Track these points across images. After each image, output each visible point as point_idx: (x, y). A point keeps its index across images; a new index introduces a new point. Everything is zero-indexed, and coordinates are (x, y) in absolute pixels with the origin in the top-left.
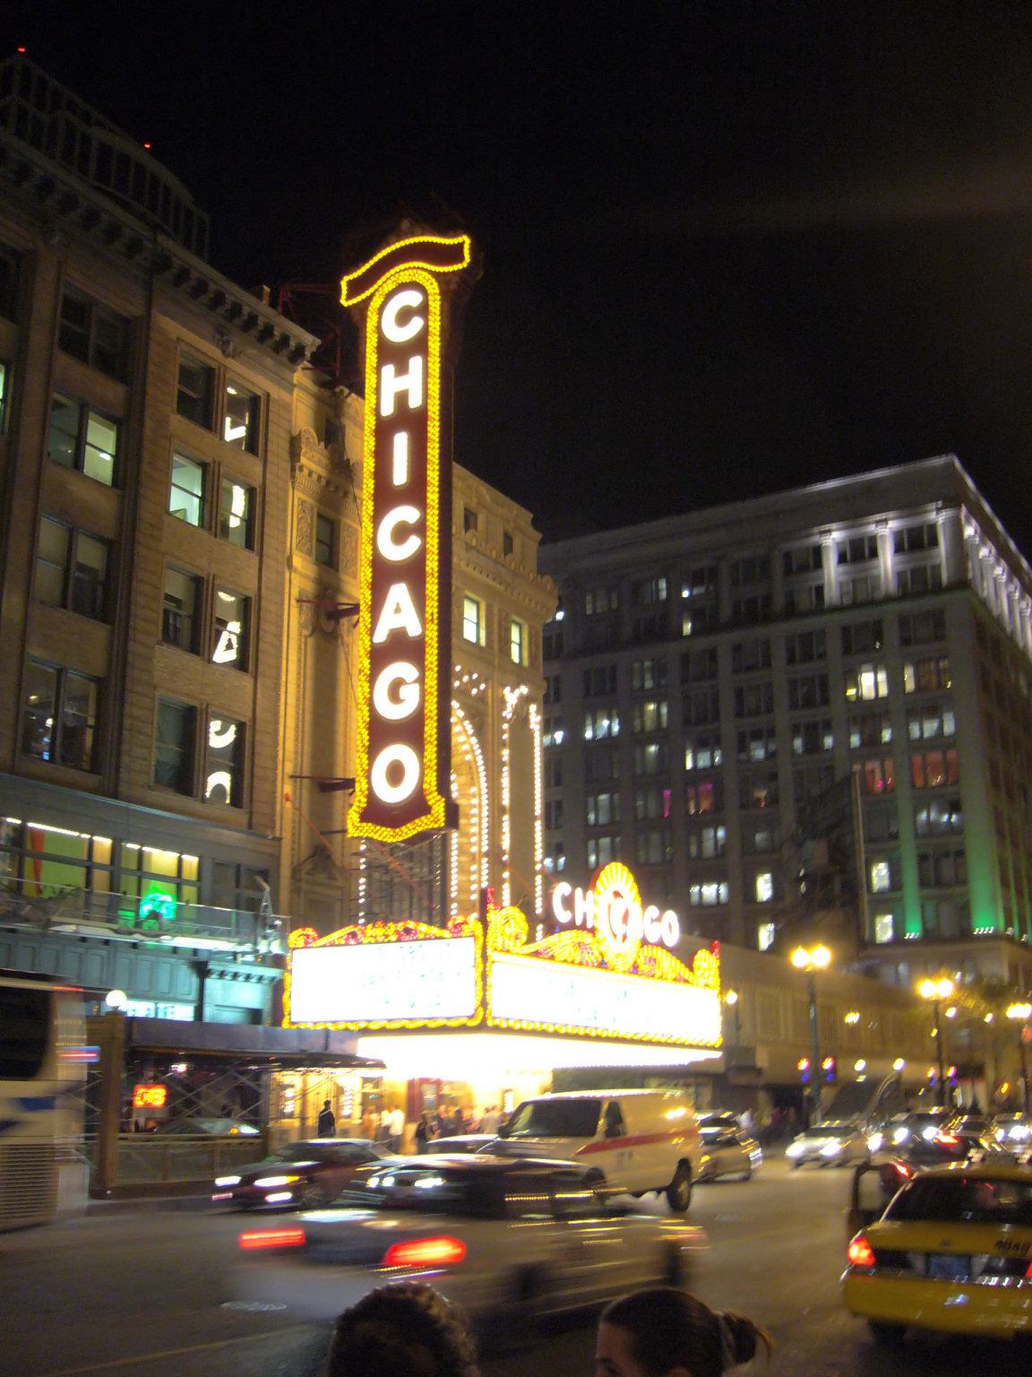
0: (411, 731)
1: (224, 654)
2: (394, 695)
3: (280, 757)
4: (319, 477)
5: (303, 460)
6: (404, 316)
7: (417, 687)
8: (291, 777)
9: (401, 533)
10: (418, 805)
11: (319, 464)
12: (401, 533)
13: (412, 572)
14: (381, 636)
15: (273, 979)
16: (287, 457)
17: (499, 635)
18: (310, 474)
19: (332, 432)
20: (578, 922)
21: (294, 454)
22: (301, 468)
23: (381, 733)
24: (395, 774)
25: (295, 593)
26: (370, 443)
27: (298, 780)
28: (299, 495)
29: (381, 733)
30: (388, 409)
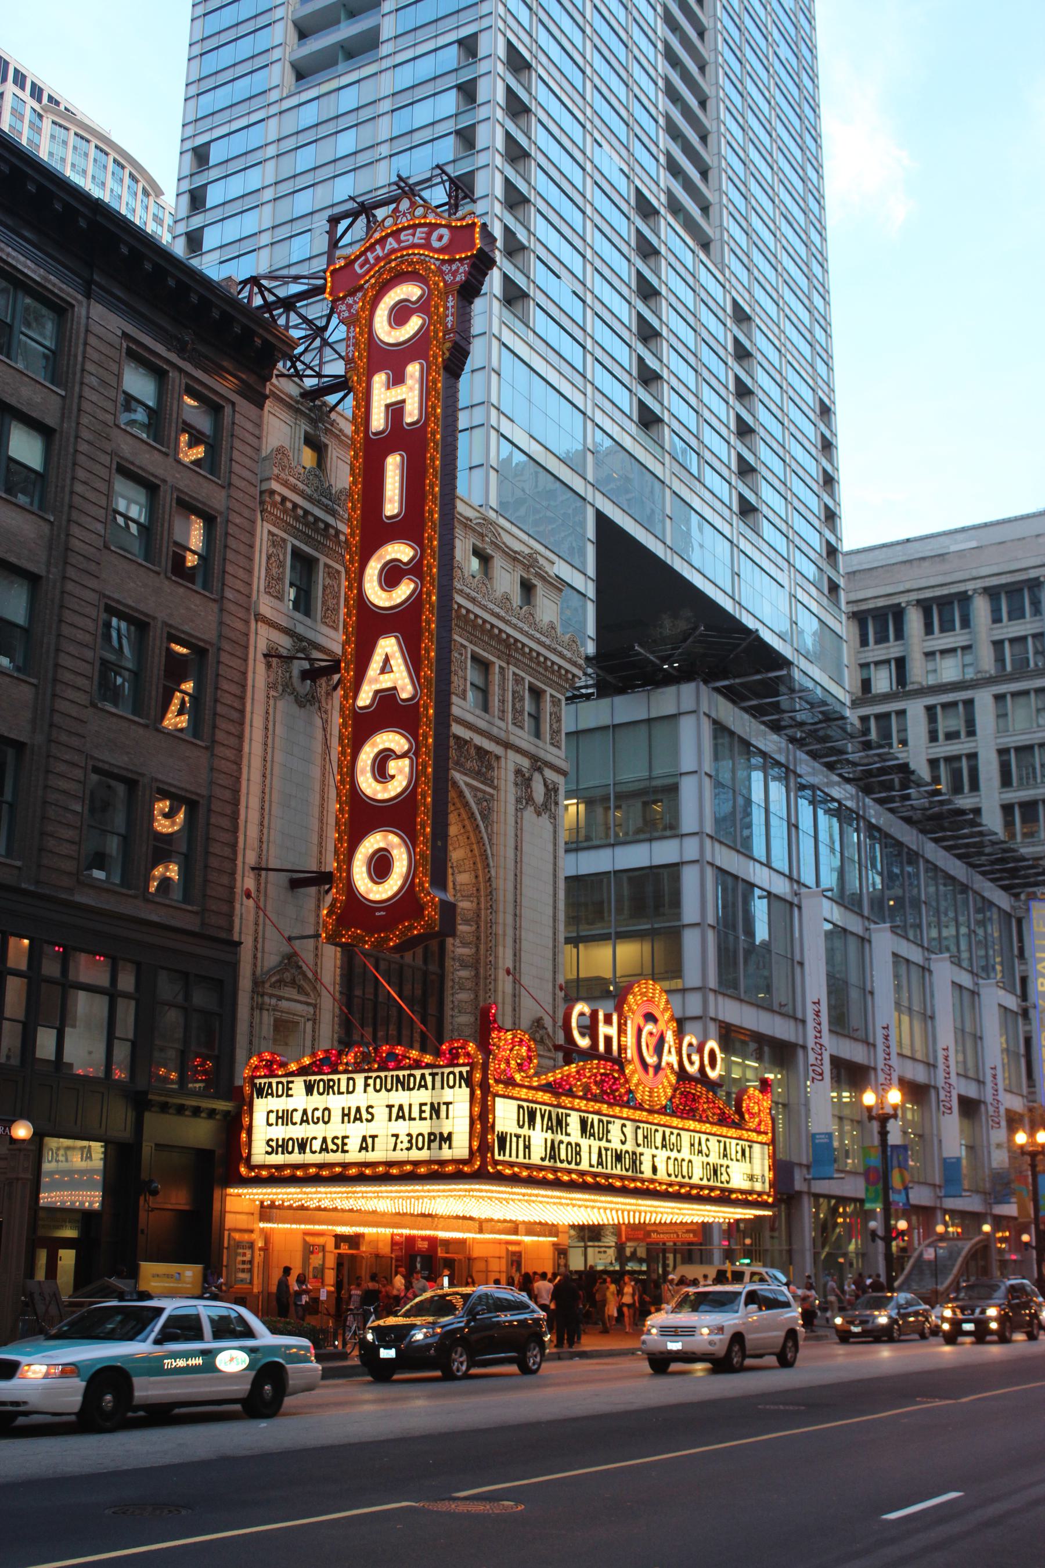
0: (396, 815)
1: (175, 720)
2: (381, 772)
3: (241, 844)
6: (400, 315)
8: (253, 869)
9: (392, 576)
10: (407, 901)
14: (365, 698)
15: (227, 1113)
17: (514, 705)
23: (364, 815)
24: (380, 866)
25: (262, 647)
27: (263, 873)
29: (364, 815)
30: (378, 421)
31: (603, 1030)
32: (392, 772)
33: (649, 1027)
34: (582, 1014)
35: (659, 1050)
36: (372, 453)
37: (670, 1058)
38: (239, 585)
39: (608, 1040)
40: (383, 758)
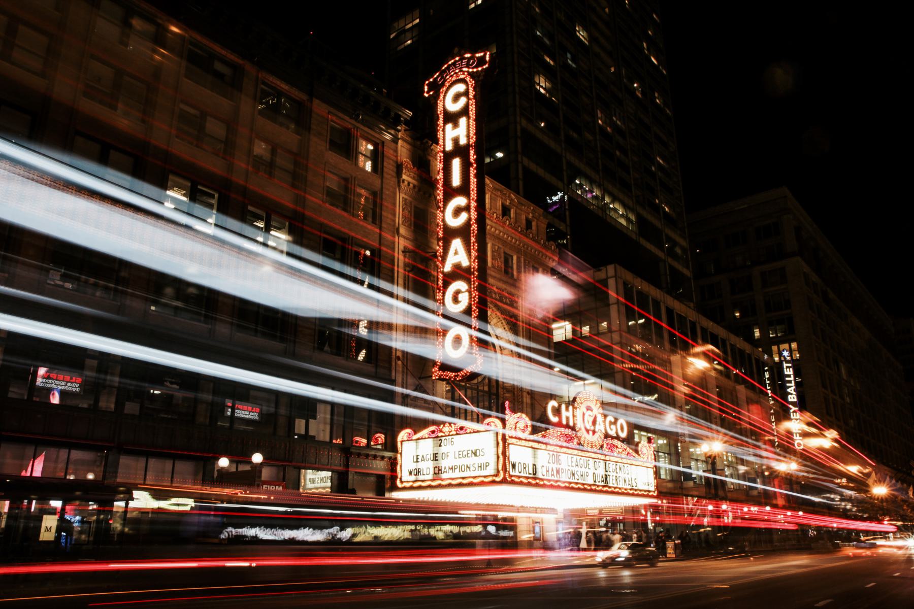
2: (456, 300)
4: (414, 186)
5: (404, 177)
7: (467, 294)
9: (457, 212)
11: (413, 178)
12: (457, 212)
13: (463, 232)
14: (448, 268)
15: (390, 458)
16: (394, 175)
18: (409, 183)
19: (422, 163)
20: (564, 422)
21: (399, 173)
22: (403, 181)
25: (401, 247)
26: (440, 166)
28: (402, 195)
30: (449, 147)
31: (564, 413)
32: (460, 299)
33: (589, 412)
34: (553, 407)
35: (594, 422)
36: (448, 157)
37: (600, 427)
38: (389, 221)
39: (568, 418)
40: (458, 292)
